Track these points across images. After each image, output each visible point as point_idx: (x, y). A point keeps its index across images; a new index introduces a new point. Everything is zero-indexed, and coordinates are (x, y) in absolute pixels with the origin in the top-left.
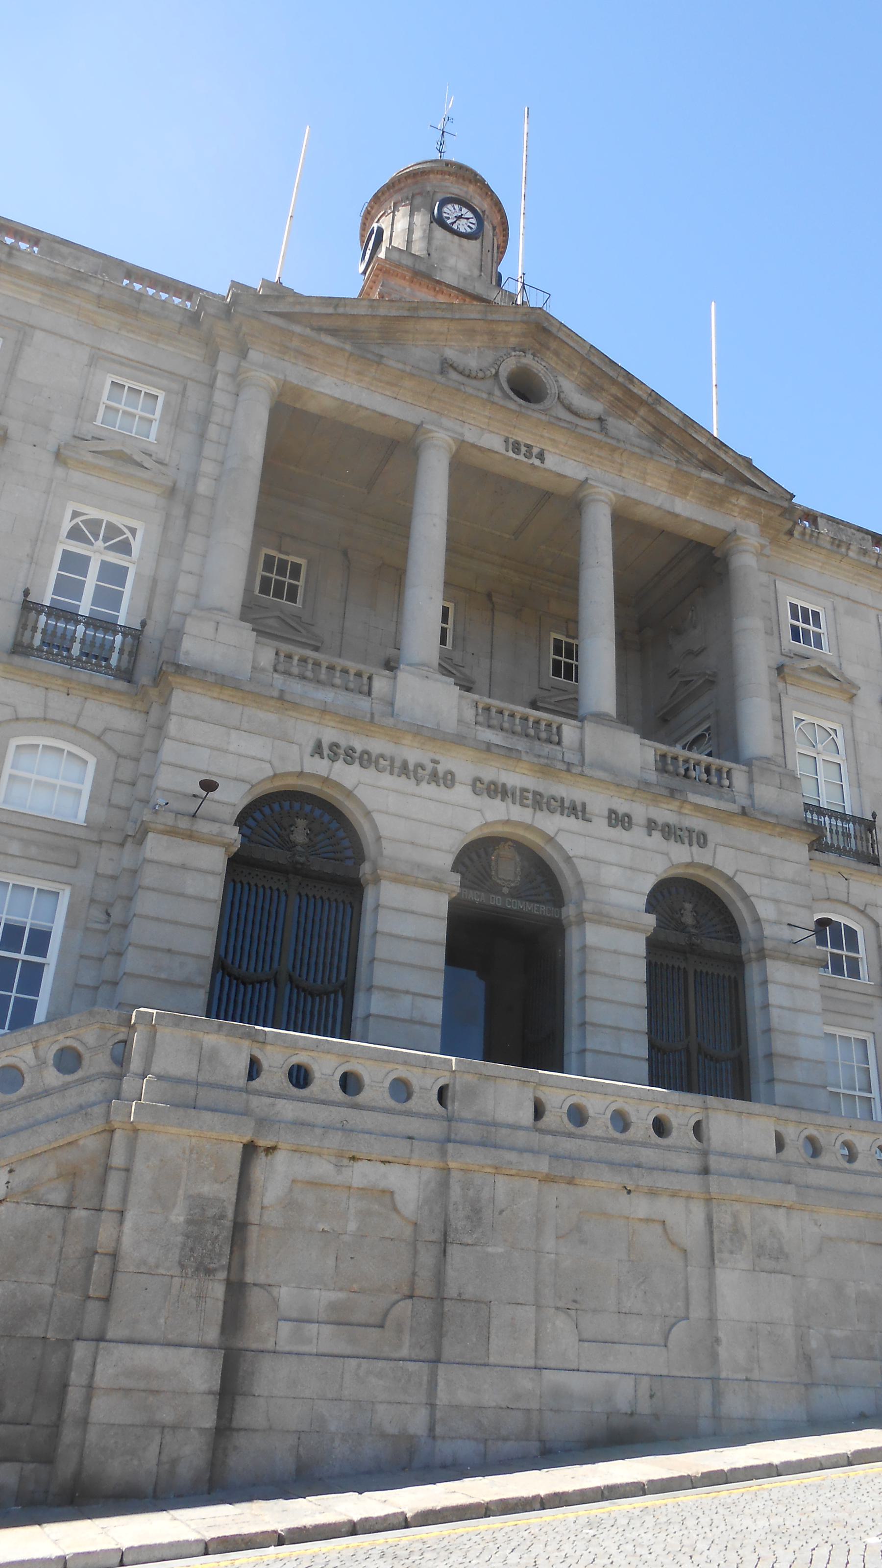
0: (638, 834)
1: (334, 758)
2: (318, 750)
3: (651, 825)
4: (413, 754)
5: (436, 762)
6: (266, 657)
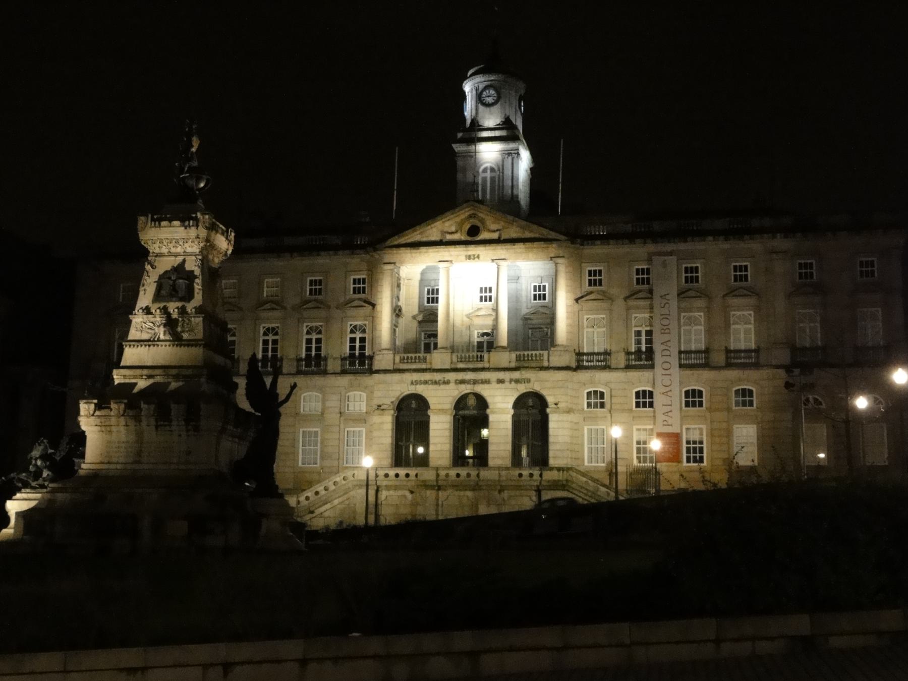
0: (507, 384)
1: (417, 384)
2: (412, 383)
3: (511, 381)
4: (438, 376)
5: (444, 378)
6: (397, 359)
